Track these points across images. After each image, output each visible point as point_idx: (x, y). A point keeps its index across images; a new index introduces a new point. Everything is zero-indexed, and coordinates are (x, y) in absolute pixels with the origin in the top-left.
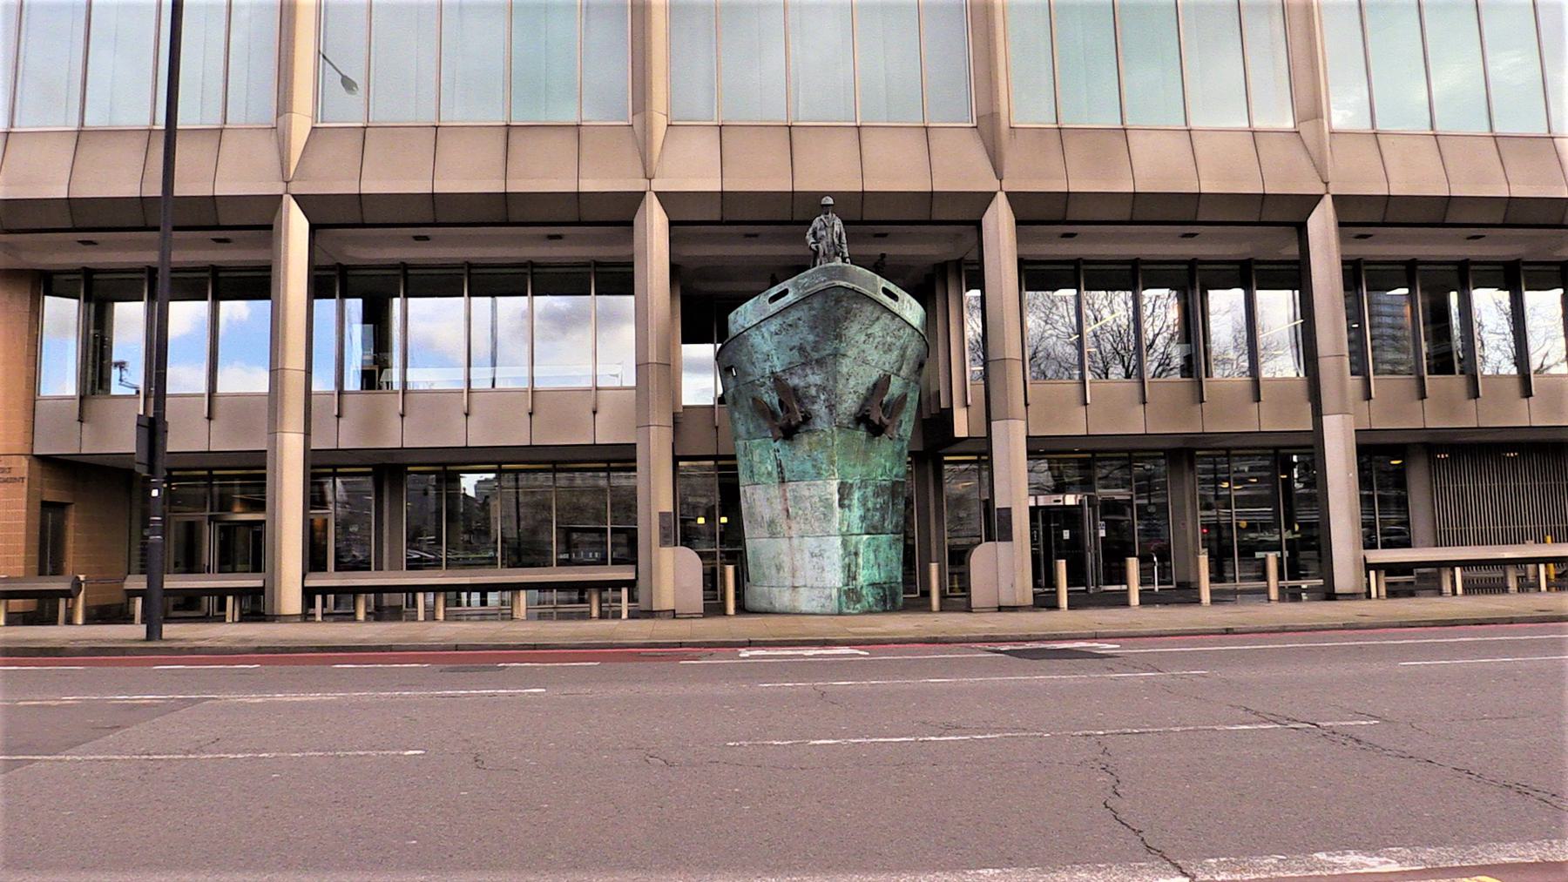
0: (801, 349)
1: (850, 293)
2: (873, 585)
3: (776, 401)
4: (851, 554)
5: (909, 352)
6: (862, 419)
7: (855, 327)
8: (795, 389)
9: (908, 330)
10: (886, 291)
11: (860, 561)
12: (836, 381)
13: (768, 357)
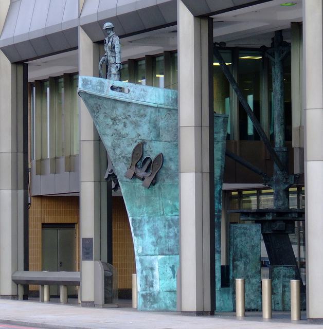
11: (156, 273)
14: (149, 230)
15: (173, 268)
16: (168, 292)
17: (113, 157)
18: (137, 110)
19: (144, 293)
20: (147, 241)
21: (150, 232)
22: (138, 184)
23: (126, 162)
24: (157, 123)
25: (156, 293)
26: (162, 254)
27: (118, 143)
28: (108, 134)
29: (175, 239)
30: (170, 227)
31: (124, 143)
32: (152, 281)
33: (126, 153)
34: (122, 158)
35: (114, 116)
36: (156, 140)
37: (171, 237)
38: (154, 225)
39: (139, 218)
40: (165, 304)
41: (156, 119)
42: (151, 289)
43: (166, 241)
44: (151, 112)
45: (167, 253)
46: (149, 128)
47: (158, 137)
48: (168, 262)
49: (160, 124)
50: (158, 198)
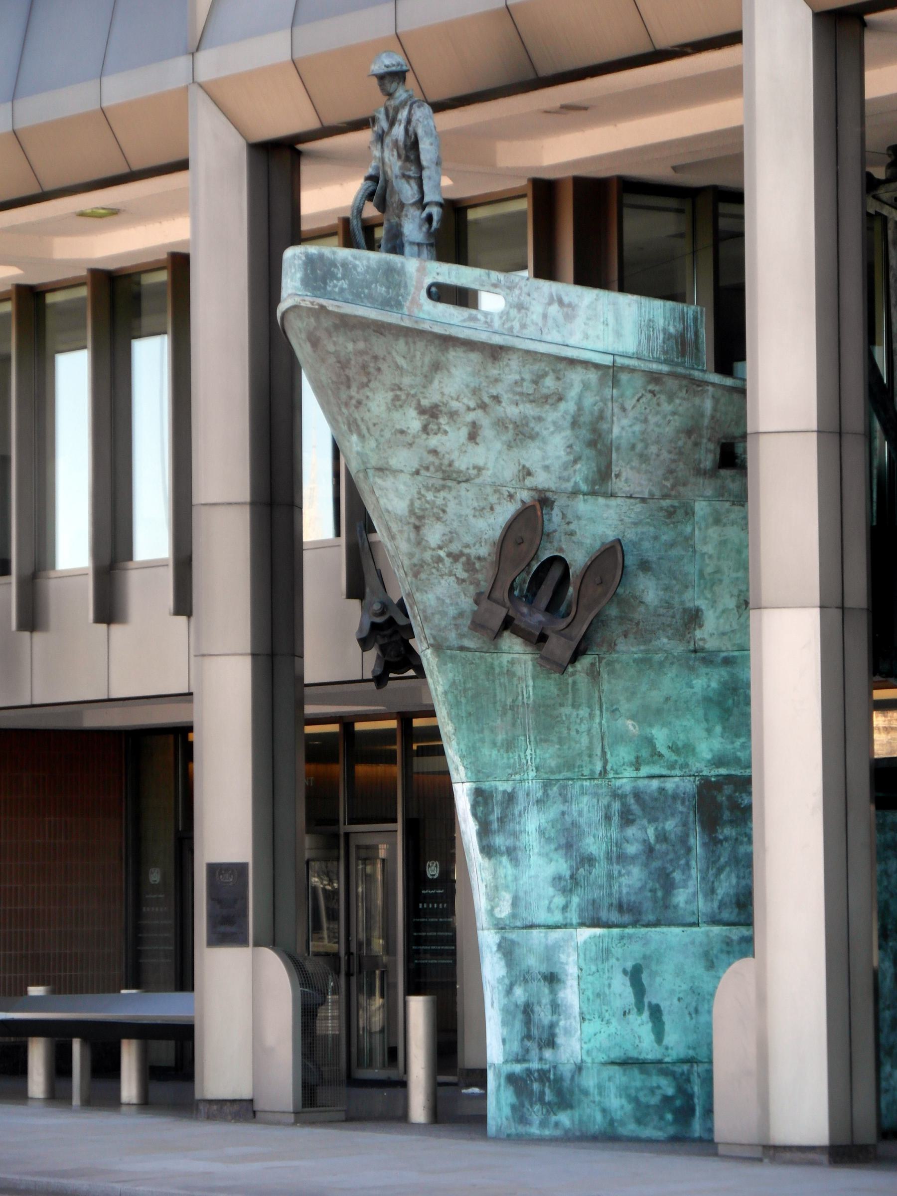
11: (570, 995)
14: (542, 832)
15: (635, 976)
16: (616, 1068)
17: (411, 555)
18: (527, 376)
19: (518, 1068)
20: (532, 873)
21: (549, 840)
22: (505, 658)
23: (464, 575)
24: (605, 426)
25: (566, 1070)
26: (596, 923)
27: (439, 502)
28: (400, 466)
29: (646, 865)
31: (460, 503)
32: (552, 1026)
33: (468, 539)
34: (448, 561)
35: (432, 397)
36: (593, 493)
37: (633, 859)
38: (563, 813)
39: (504, 786)
40: (604, 1111)
41: (602, 411)
42: (548, 1054)
43: (610, 876)
44: (586, 386)
45: (614, 917)
46: (570, 446)
47: (601, 482)
48: (617, 951)
49: (616, 431)
50: (584, 712)
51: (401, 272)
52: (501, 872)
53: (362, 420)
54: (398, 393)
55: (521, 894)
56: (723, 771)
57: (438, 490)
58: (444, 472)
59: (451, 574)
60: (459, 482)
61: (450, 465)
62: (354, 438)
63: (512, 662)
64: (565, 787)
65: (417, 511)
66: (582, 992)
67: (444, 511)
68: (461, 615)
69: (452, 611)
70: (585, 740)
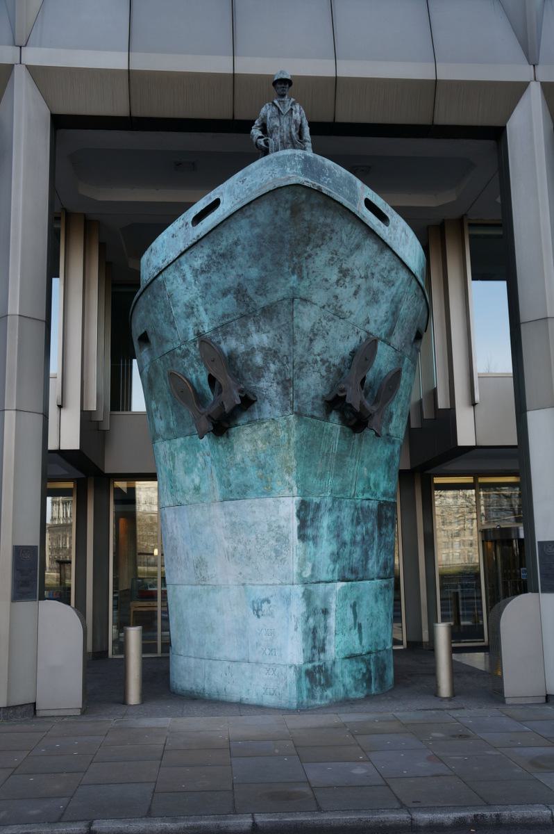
0: (240, 292)
1: (315, 200)
2: (351, 657)
3: (204, 378)
4: (317, 612)
5: (403, 310)
6: (335, 403)
7: (322, 257)
8: (231, 359)
9: (403, 275)
10: (369, 204)
11: (332, 621)
12: (293, 342)
13: (190, 310)
14: (329, 528)
16: (347, 660)
17: (302, 356)
19: (310, 666)
20: (323, 551)
21: (331, 531)
22: (330, 425)
25: (329, 665)
26: (343, 580)
27: (327, 327)
28: (317, 301)
29: (362, 547)
30: (358, 523)
31: (337, 330)
32: (324, 640)
33: (333, 353)
34: (320, 363)
38: (338, 517)
39: (316, 500)
40: (344, 686)
42: (322, 656)
43: (351, 554)
48: (349, 595)
50: (353, 461)
51: (355, 185)
52: (308, 550)
53: (307, 267)
54: (334, 256)
55: (316, 563)
56: (384, 499)
57: (329, 320)
58: (336, 310)
59: (319, 371)
60: (340, 318)
61: (340, 307)
62: (295, 277)
63: (332, 428)
64: (340, 502)
65: (315, 330)
66: (336, 619)
67: (328, 334)
68: (317, 397)
69: (313, 394)
70: (351, 477)
